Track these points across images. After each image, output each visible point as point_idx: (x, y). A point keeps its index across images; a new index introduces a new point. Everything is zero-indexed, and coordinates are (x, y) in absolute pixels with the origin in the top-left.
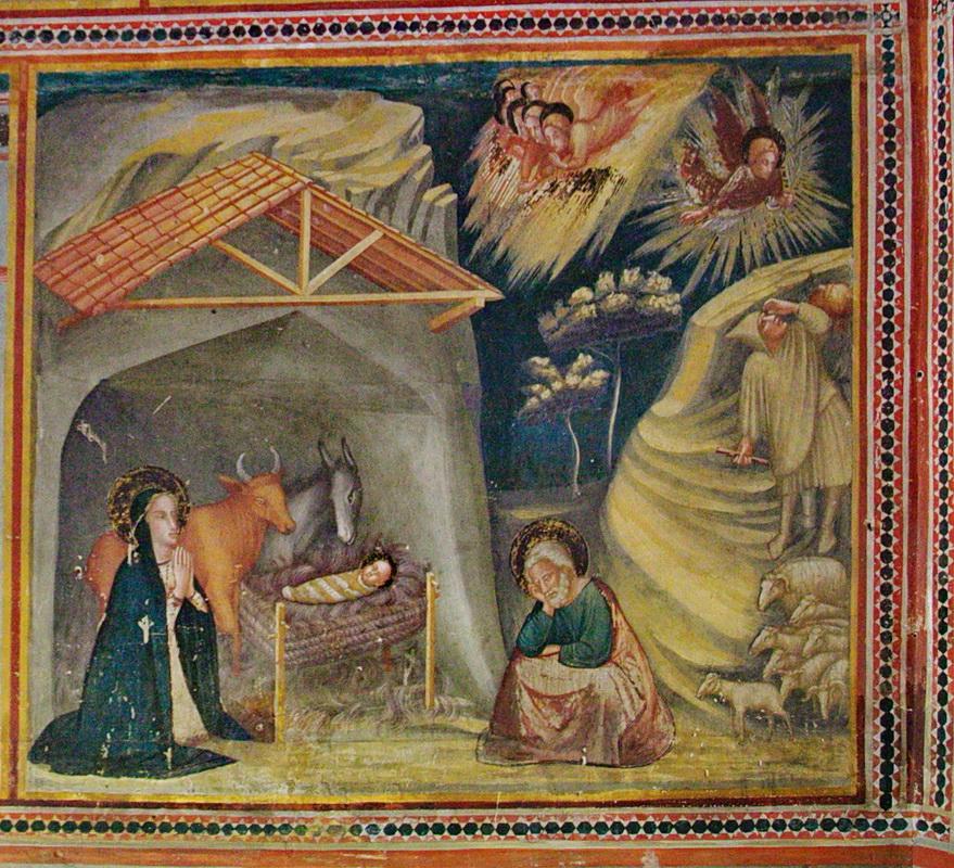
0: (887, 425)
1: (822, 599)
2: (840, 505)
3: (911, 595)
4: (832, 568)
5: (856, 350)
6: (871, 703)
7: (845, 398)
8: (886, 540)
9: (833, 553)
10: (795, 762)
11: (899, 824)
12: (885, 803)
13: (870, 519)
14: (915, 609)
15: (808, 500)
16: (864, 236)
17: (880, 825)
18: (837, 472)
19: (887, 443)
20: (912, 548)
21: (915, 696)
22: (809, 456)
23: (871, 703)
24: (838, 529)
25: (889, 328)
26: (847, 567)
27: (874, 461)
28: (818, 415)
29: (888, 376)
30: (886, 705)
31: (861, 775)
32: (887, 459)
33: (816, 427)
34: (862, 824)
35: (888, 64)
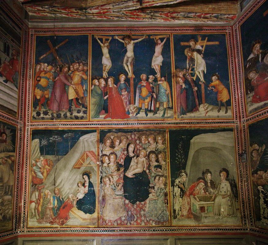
0: (18, 177)
1: (8, 201)
2: (11, 188)
3: (20, 200)
4: (10, 197)
5: (15, 167)
6: (14, 216)
7: (13, 173)
8: (17, 193)
9: (11, 195)
10: (3, 227)
11: (17, 232)
12: (15, 230)
13: (16, 190)
14: (21, 202)
15: (7, 187)
16: (17, 152)
17: (15, 233)
18: (12, 183)
19: (18, 180)
20: (20, 194)
21: (20, 214)
22: (8, 181)
23: (14, 216)
24: (11, 192)
25: (19, 164)
26: (12, 197)
27: (16, 182)
28: (9, 175)
29: (19, 171)
30: (16, 216)
31: (12, 227)
32: (18, 182)
33: (9, 176)
34: (12, 234)
35: (21, 130)
